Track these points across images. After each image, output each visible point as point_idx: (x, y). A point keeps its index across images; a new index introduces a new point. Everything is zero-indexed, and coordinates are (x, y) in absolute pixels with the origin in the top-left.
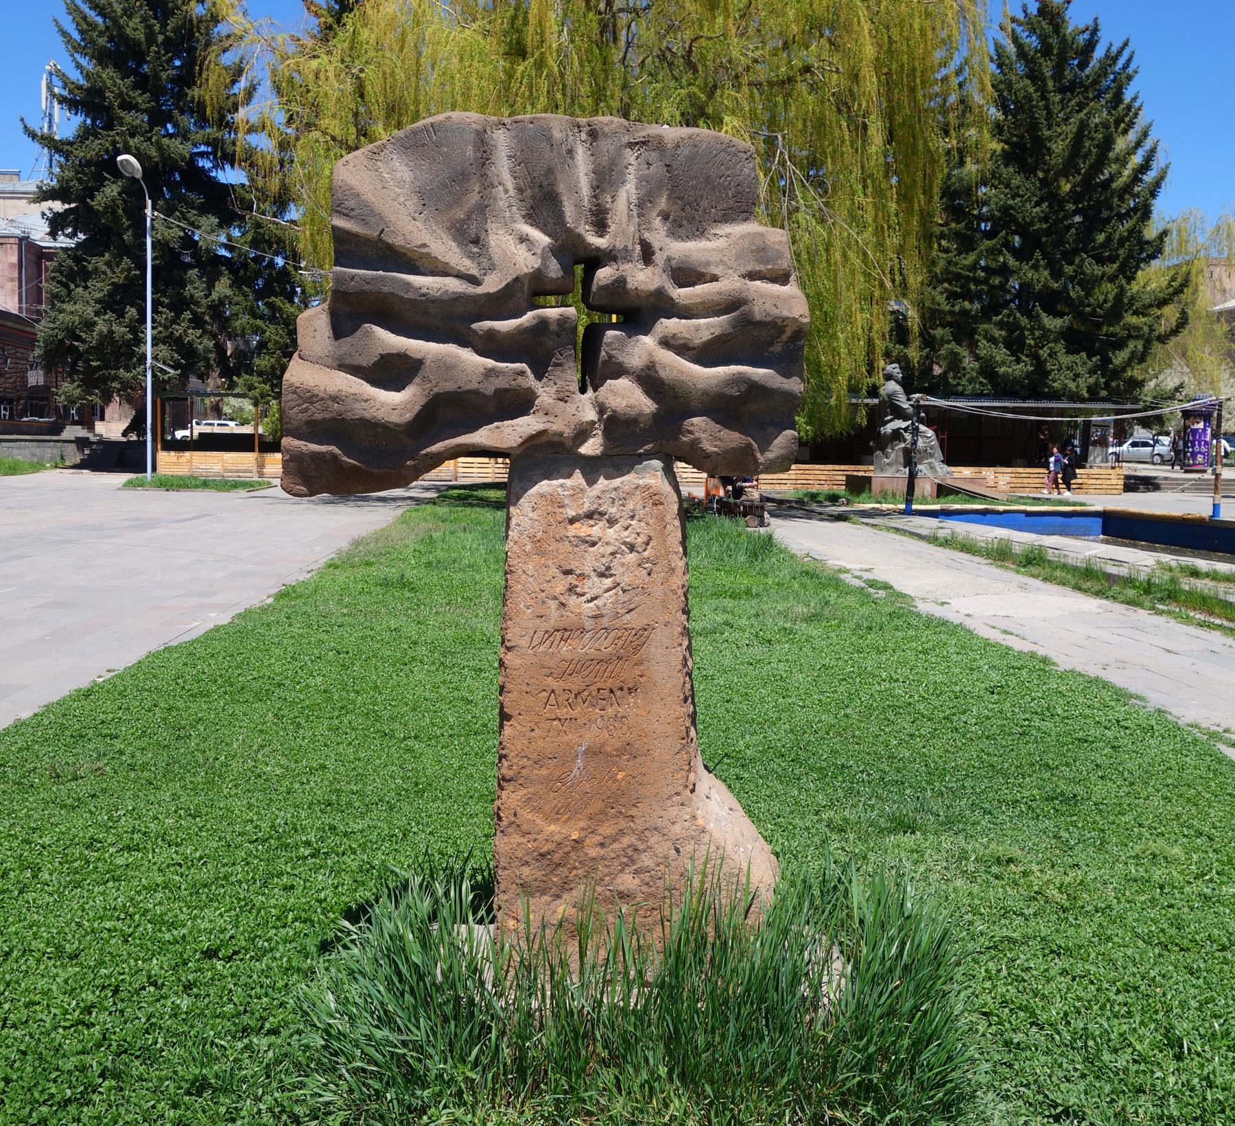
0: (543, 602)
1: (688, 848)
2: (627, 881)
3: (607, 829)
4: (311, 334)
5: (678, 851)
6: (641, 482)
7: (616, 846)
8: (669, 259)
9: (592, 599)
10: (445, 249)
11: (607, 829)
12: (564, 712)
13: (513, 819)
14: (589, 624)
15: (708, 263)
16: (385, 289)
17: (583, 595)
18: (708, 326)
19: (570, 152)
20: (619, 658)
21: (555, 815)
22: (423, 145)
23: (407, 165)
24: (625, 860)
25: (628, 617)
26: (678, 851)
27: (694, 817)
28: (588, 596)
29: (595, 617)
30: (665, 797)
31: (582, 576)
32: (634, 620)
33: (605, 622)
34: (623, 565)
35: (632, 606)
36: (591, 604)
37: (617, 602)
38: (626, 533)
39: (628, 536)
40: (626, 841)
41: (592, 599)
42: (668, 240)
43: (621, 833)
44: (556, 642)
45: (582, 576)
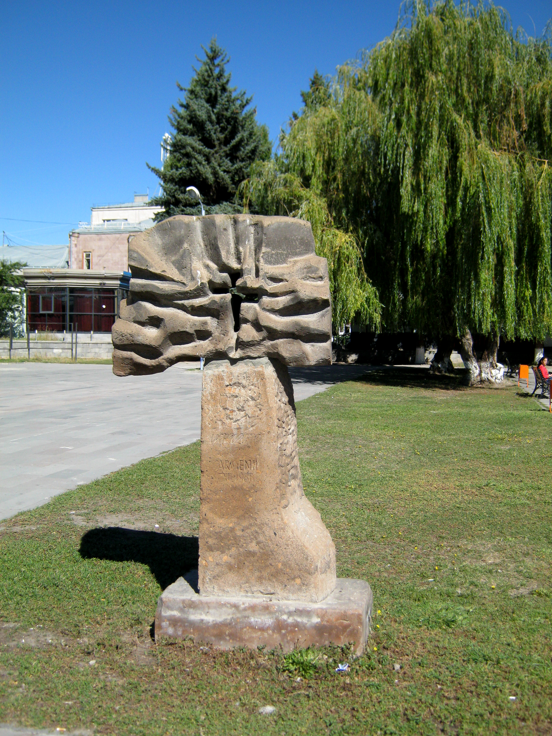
0: (216, 422)
2: (253, 547)
5: (275, 534)
6: (256, 369)
7: (249, 531)
8: (266, 273)
9: (236, 421)
10: (172, 272)
11: (245, 524)
12: (225, 471)
14: (235, 432)
15: (283, 274)
16: (149, 290)
17: (232, 419)
19: (225, 229)
20: (249, 447)
21: (222, 516)
22: (166, 230)
24: (252, 537)
25: (251, 429)
26: (275, 534)
27: (282, 519)
29: (238, 429)
31: (233, 411)
33: (242, 431)
34: (249, 406)
35: (253, 424)
36: (236, 423)
37: (246, 421)
38: (250, 392)
39: (250, 393)
41: (236, 421)
42: (266, 265)
45: (233, 411)
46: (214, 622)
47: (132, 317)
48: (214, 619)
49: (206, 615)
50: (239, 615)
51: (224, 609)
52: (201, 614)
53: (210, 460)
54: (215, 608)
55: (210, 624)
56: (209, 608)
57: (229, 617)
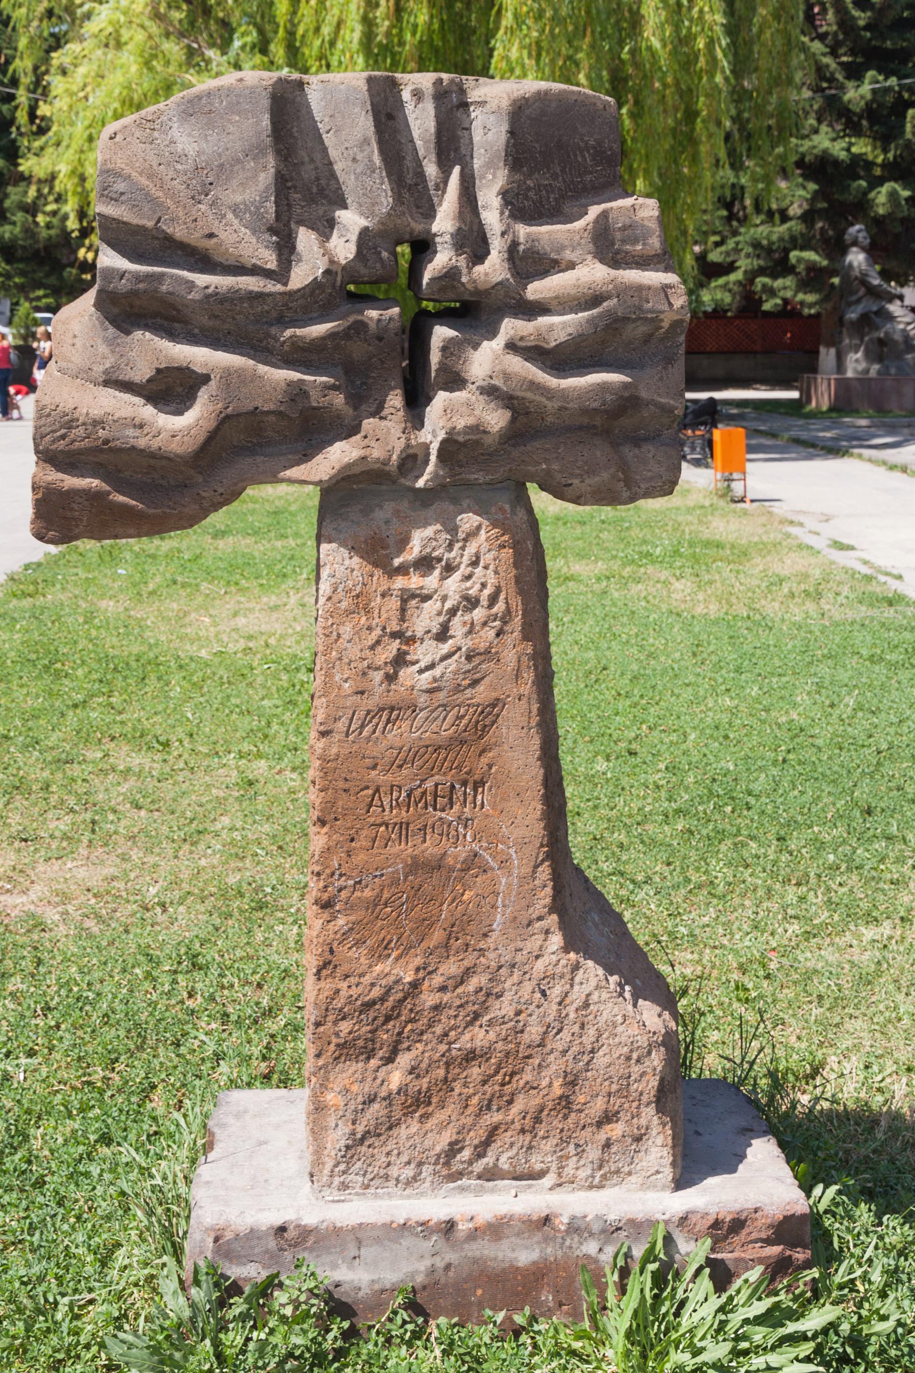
1: (556, 992)
3: (451, 968)
4: (70, 341)
11: (451, 968)
13: (328, 956)
14: (423, 700)
15: (563, 248)
18: (565, 325)
23: (189, 135)
26: (544, 994)
28: (422, 664)
30: (525, 922)
31: (411, 640)
32: (482, 694)
35: (478, 676)
40: (473, 983)
43: (468, 973)
44: (381, 726)
46: (377, 1287)
47: (99, 369)
48: (375, 1277)
49: (351, 1267)
50: (451, 1256)
51: (407, 1241)
52: (334, 1266)
53: (346, 786)
54: (378, 1240)
55: (361, 1294)
56: (359, 1243)
57: (423, 1266)
